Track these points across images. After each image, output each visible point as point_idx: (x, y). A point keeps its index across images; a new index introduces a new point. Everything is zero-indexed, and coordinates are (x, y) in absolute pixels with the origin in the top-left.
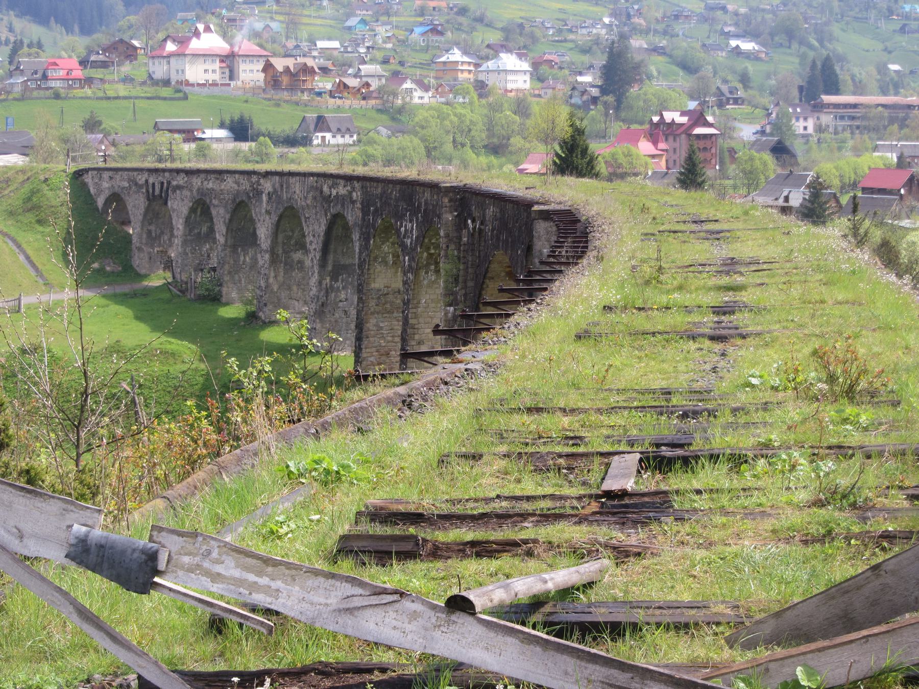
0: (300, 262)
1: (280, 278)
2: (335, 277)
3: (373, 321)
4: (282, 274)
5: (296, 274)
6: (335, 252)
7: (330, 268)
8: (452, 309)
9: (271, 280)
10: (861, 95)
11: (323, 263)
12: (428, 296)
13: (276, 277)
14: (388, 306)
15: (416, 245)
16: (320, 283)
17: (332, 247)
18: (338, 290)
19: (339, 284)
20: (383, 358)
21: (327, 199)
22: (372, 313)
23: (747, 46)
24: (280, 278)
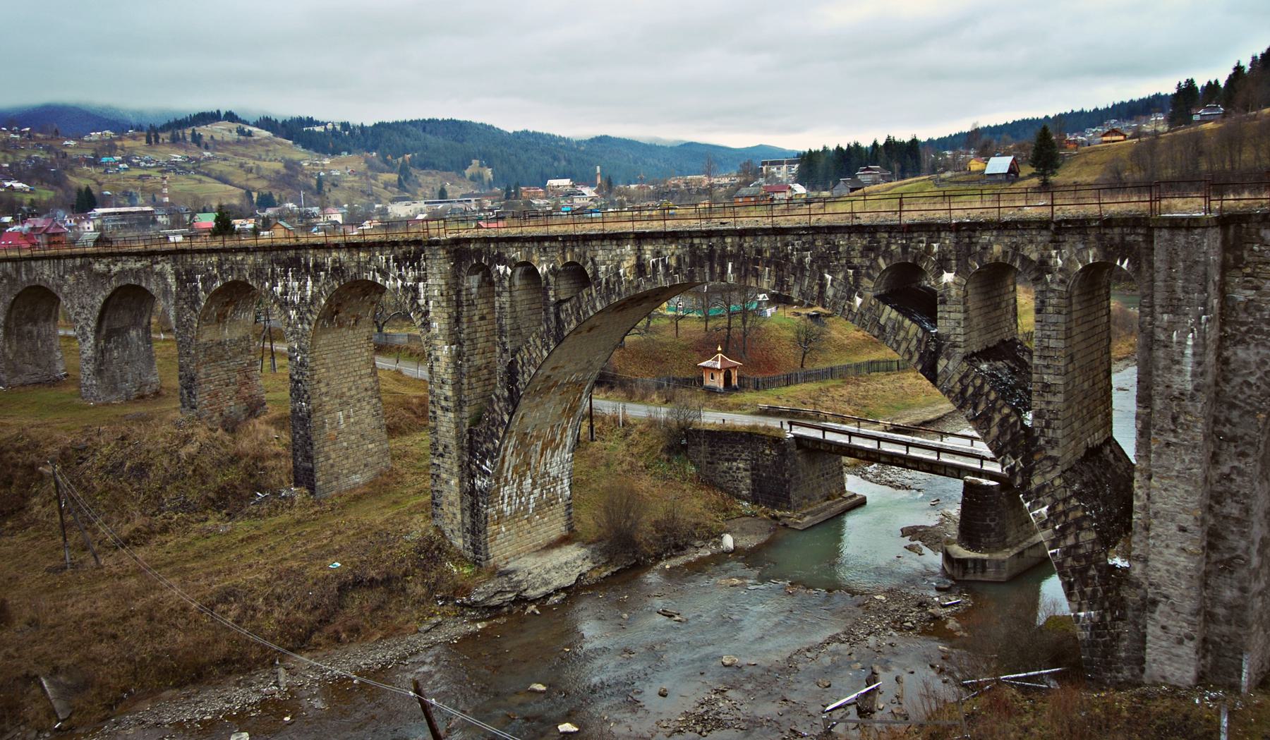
0: (30, 332)
1: (14, 348)
2: (108, 340)
3: (203, 370)
4: (15, 344)
5: (27, 343)
6: (109, 318)
7: (104, 332)
8: (454, 347)
9: (7, 350)
10: (132, 206)
11: (98, 331)
12: (321, 342)
13: (10, 347)
14: (213, 356)
15: (315, 298)
16: (96, 346)
17: (107, 314)
18: (111, 350)
19: (112, 345)
20: (214, 400)
21: (106, 276)
22: (202, 364)
23: (17, 185)
24: (14, 348)
